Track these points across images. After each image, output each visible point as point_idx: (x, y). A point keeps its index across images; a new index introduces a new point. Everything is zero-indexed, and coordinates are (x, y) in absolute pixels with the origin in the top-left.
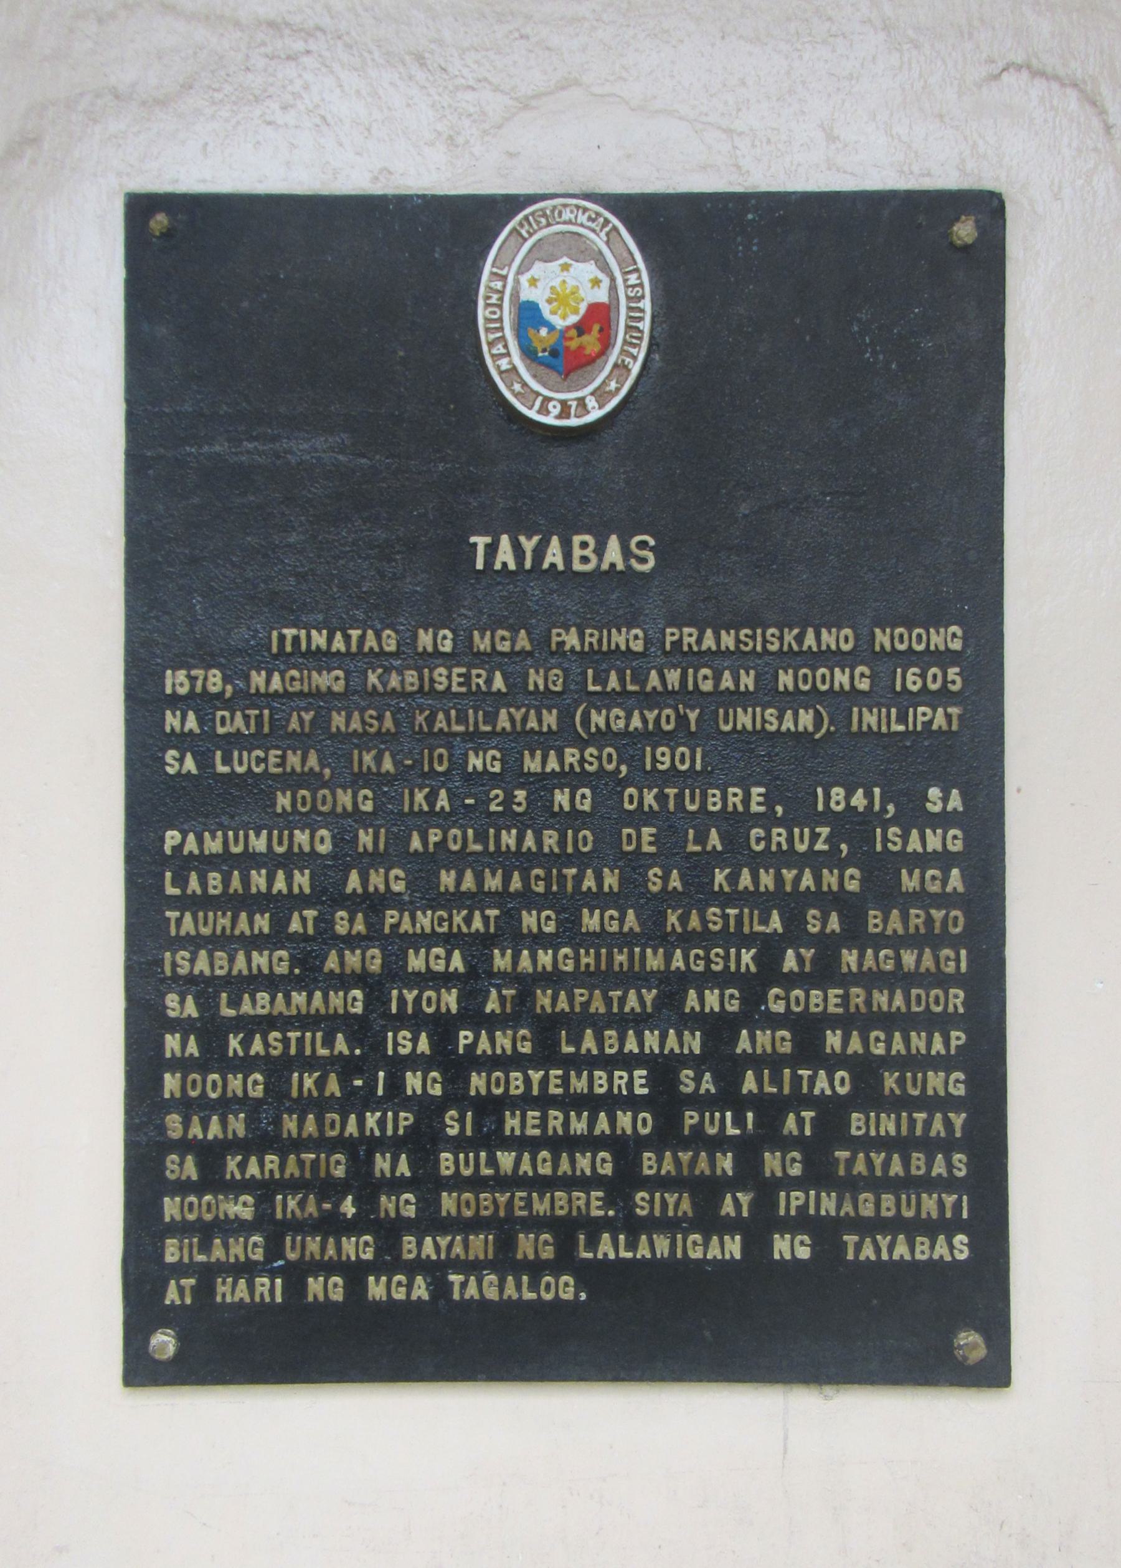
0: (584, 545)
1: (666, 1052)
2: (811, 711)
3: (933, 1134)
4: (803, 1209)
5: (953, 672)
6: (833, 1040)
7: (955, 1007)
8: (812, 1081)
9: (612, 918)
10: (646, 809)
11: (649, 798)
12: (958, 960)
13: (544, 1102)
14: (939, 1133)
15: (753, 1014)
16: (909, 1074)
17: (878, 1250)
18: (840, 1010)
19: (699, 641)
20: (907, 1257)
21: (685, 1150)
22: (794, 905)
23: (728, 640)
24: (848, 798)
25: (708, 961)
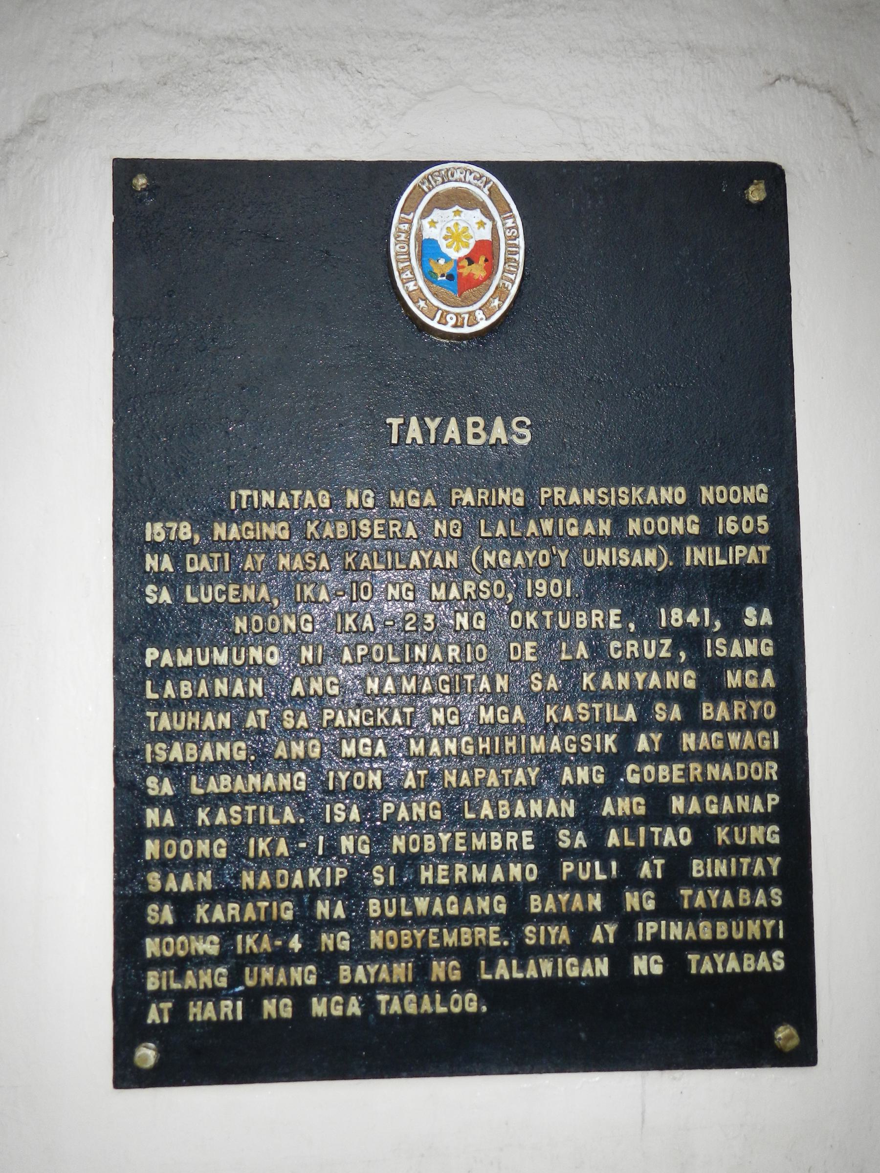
0: (476, 425)
1: (548, 816)
2: (654, 551)
3: (756, 873)
4: (656, 936)
5: (761, 519)
6: (677, 804)
7: (771, 775)
8: (661, 836)
9: (503, 712)
10: (528, 626)
11: (531, 619)
12: (772, 739)
13: (451, 856)
14: (760, 873)
15: (614, 786)
16: (736, 829)
17: (714, 965)
18: (682, 780)
19: (566, 498)
20: (738, 970)
21: (563, 892)
22: (645, 699)
23: (589, 497)
24: (684, 617)
25: (579, 743)
